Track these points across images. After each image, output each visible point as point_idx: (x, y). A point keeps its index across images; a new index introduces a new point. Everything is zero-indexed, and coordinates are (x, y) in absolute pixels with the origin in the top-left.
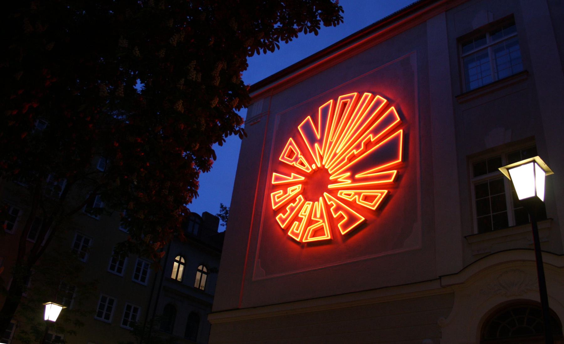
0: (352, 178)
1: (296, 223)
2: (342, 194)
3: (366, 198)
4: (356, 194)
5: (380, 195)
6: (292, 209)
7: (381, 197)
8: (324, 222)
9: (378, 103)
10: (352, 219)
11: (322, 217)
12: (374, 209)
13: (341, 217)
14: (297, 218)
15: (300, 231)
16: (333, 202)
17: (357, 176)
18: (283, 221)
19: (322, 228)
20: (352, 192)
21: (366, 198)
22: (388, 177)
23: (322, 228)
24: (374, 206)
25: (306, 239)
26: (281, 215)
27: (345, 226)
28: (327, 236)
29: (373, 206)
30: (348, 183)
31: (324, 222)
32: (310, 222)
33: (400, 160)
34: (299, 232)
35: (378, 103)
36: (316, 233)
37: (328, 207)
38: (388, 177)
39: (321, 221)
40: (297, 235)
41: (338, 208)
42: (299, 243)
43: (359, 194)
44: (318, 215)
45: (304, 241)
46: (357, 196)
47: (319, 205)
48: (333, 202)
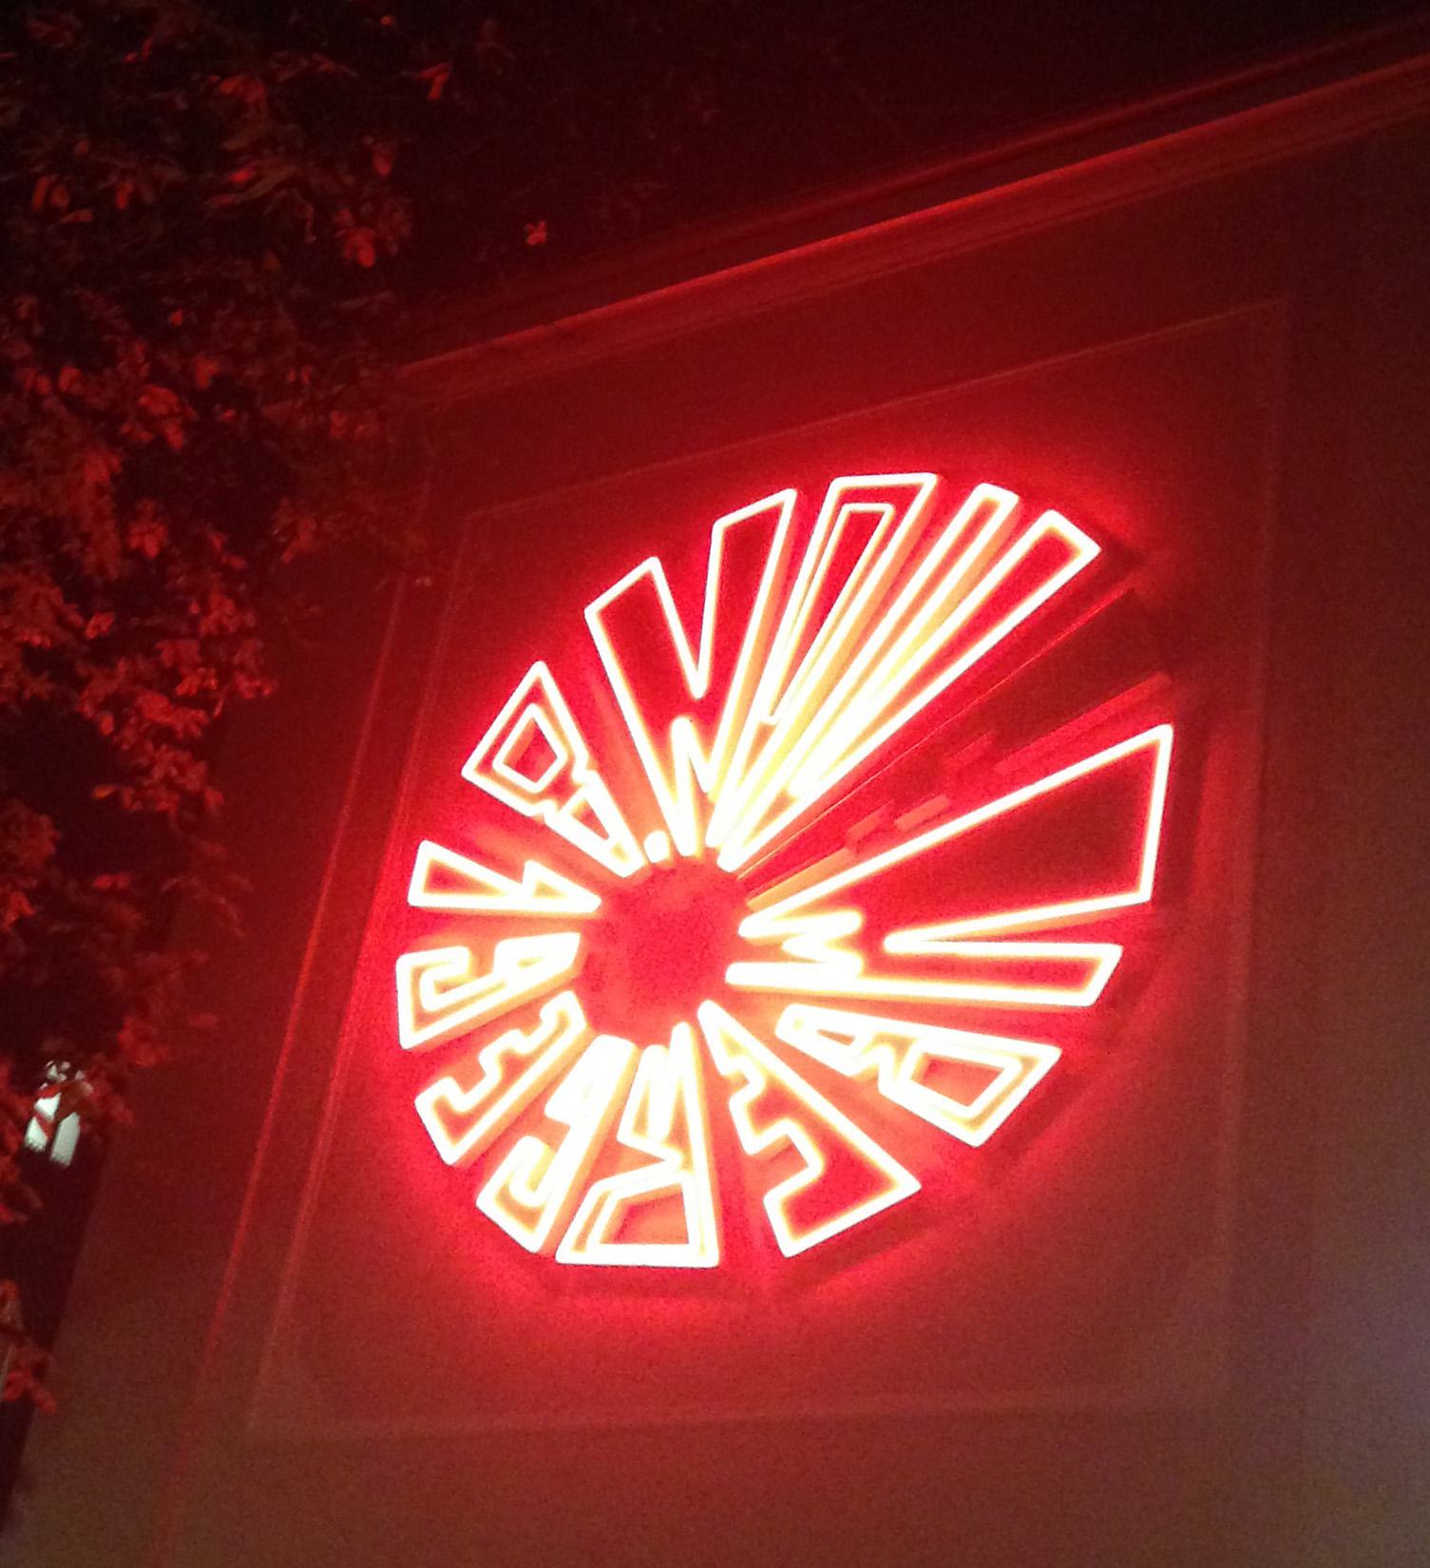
0: (869, 940)
1: (527, 1149)
2: (797, 1026)
3: (935, 1071)
4: (882, 1039)
5: (1022, 1066)
6: (514, 1067)
7: (1016, 1083)
8: (688, 1164)
9: (1051, 552)
10: (847, 1177)
11: (679, 1136)
12: (976, 1138)
13: (787, 1156)
14: (530, 1118)
15: (551, 1198)
16: (751, 1065)
17: (901, 942)
18: (458, 1125)
19: (669, 1202)
20: (864, 1026)
21: (935, 1071)
22: (1072, 974)
23: (669, 1202)
24: (977, 1122)
25: (581, 1243)
26: (775, 1204)
27: (806, 1210)
28: (700, 1247)
29: (972, 1122)
30: (849, 973)
31: (688, 1164)
32: (608, 1157)
33: (1143, 892)
34: (534, 1200)
35: (1051, 552)
36: (632, 1221)
37: (717, 1090)
38: (1072, 974)
39: (673, 1155)
40: (530, 1217)
41: (773, 1105)
42: (543, 1263)
43: (901, 1046)
44: (661, 1123)
45: (566, 1255)
46: (887, 1051)
47: (667, 1072)
48: (751, 1065)
